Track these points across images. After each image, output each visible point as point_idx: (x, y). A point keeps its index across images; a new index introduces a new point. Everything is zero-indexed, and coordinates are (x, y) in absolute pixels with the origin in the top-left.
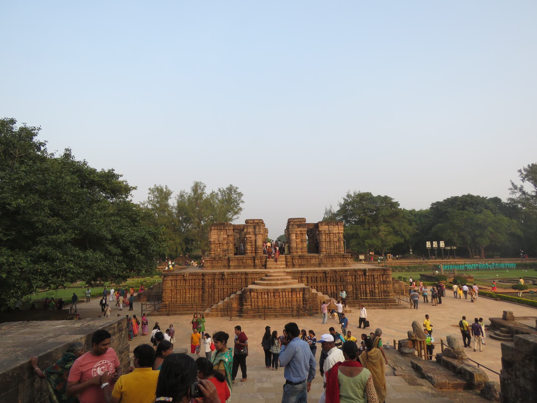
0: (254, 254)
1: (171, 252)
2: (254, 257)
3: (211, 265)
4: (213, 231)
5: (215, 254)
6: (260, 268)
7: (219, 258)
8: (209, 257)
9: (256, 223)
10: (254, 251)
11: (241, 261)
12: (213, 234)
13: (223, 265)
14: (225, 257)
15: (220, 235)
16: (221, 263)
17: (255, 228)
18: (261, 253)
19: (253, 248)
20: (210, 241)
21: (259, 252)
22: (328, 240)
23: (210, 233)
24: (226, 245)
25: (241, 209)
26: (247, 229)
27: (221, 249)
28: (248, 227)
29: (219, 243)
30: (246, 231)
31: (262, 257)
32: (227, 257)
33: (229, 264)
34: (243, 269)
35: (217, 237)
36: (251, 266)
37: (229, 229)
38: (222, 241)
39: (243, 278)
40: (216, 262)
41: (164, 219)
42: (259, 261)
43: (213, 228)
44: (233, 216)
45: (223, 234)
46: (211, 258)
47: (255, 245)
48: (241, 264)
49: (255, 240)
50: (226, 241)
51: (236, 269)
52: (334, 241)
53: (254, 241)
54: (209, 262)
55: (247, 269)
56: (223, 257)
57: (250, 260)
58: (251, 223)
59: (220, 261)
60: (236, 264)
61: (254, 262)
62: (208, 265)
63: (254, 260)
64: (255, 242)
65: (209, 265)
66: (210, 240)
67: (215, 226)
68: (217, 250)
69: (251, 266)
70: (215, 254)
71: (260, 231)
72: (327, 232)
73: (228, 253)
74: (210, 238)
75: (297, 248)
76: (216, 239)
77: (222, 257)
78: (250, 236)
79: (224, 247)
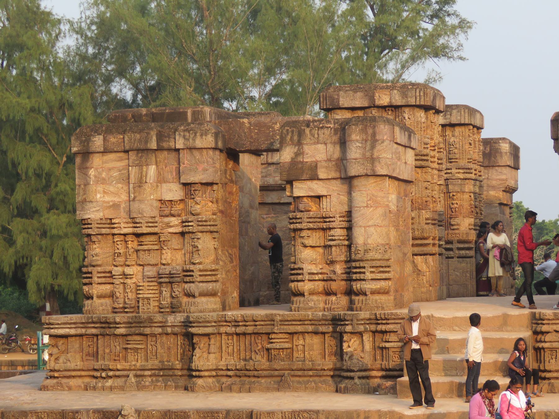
0: (344, 300)
1: (55, 276)
2: (336, 321)
4: (96, 161)
5: (112, 295)
6: (373, 391)
7: (129, 324)
8: (75, 317)
9: (384, 108)
10: (339, 285)
11: (262, 342)
12: (100, 180)
13: (154, 363)
14: (171, 319)
15: (141, 183)
16: (142, 355)
17: (343, 143)
18: (383, 298)
19: (332, 263)
20: (84, 223)
21: (368, 286)
23: (84, 169)
24: (176, 242)
25: (464, 25)
26: (299, 143)
27: (151, 272)
28: (301, 134)
29: (138, 235)
30: (294, 162)
31: (386, 319)
32: (180, 317)
33: (191, 360)
34: (268, 389)
35: (124, 197)
36: (318, 373)
37: (191, 149)
38: (153, 222)
40: (117, 346)
41: (19, 94)
42: (368, 346)
43: (98, 141)
44: (404, 67)
45: (161, 180)
46: (85, 325)
47: (349, 247)
48: (261, 361)
49: (349, 214)
50: (174, 221)
51: (230, 389)
53: (338, 222)
54: (75, 344)
55: (296, 390)
56: (158, 318)
57: (316, 340)
58: (353, 109)
59: (136, 342)
60: (232, 362)
61: (340, 353)
62: (71, 365)
63: (339, 337)
64: (349, 229)
65: (79, 364)
66: (81, 215)
67: (108, 131)
68: (125, 276)
69: (318, 373)
70: (112, 295)
71: (373, 160)
73: (190, 295)
74: (84, 201)
76: (115, 206)
77: (150, 320)
78: (318, 188)
79: (167, 256)
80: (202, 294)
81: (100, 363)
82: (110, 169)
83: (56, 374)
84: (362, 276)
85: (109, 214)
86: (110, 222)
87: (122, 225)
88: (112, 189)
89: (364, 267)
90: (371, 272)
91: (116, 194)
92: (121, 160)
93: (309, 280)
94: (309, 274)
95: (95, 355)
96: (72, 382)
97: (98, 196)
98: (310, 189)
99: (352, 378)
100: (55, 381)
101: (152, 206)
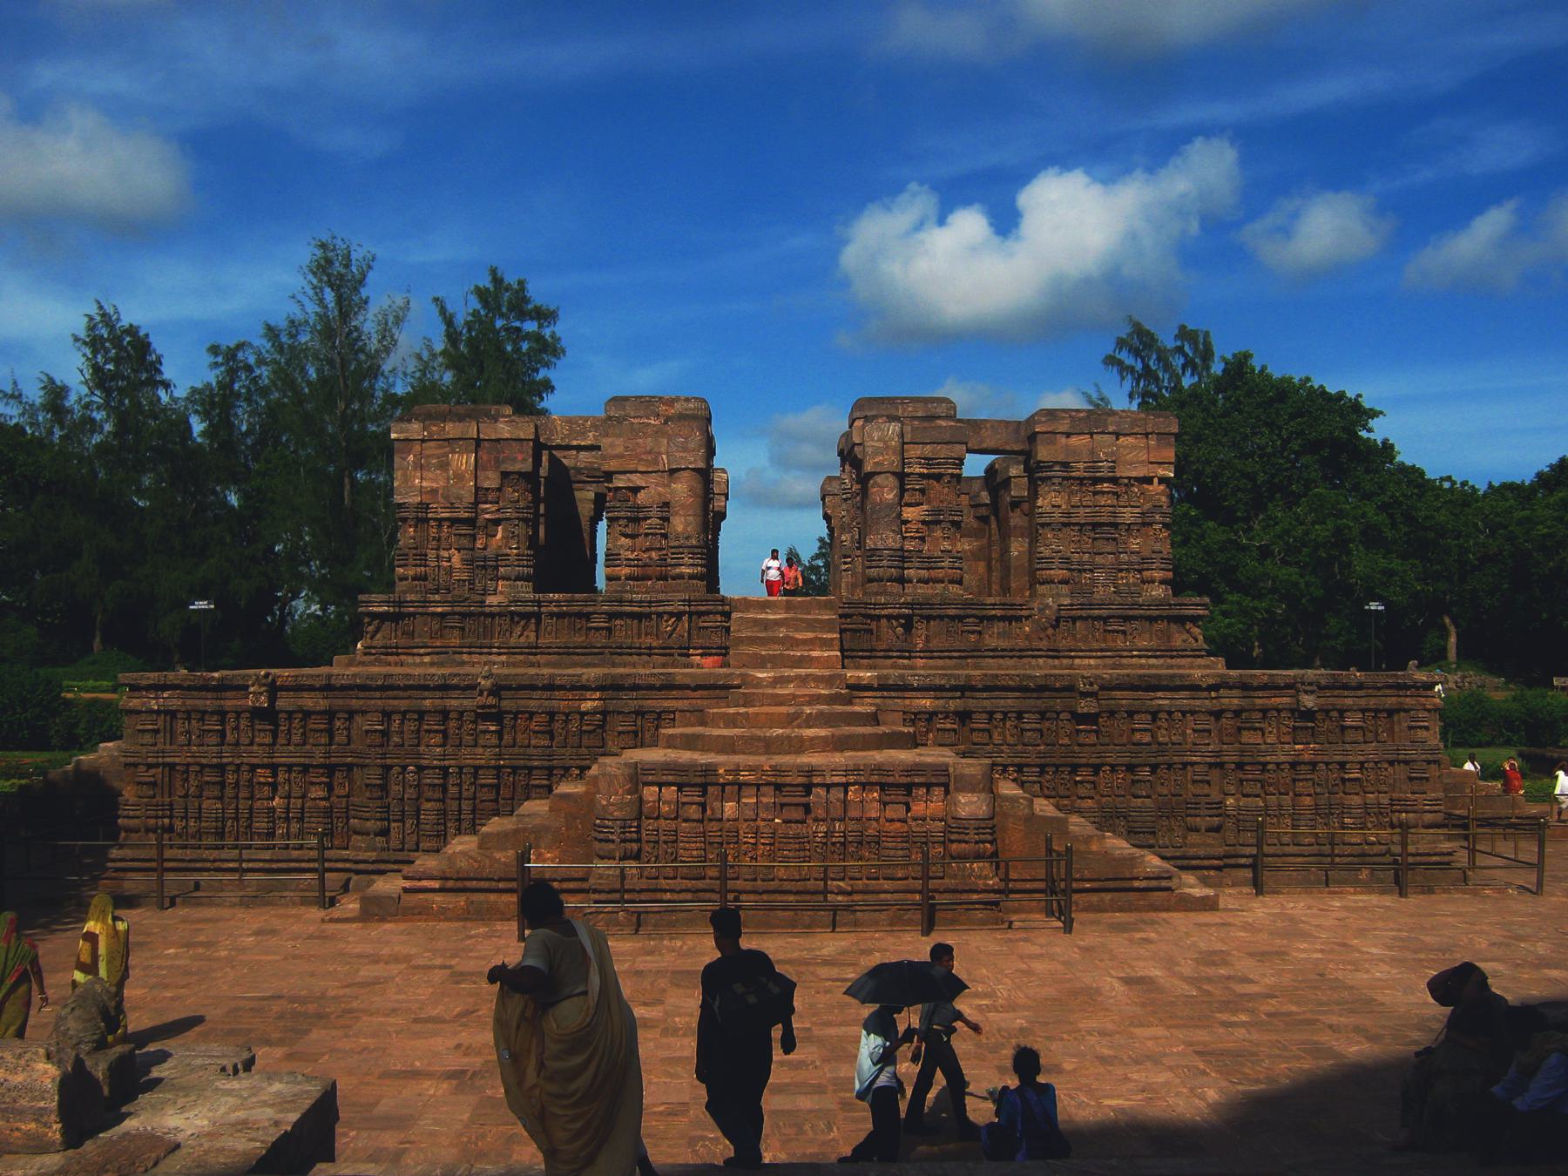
3: (403, 642)
22: (1081, 515)
39: (593, 713)
50: (494, 508)
52: (1115, 525)
72: (1079, 470)
75: (903, 559)
76: (434, 491)
80: (518, 578)
81: (416, 640)
82: (429, 456)
83: (373, 651)
84: (681, 561)
85: (426, 499)
86: (424, 506)
87: (440, 510)
88: (430, 475)
89: (683, 553)
90: (690, 558)
91: (435, 480)
92: (441, 447)
93: (626, 566)
94: (626, 559)
95: (412, 635)
96: (390, 658)
97: (417, 481)
98: (629, 480)
99: (672, 655)
100: (373, 657)
101: (471, 491)
